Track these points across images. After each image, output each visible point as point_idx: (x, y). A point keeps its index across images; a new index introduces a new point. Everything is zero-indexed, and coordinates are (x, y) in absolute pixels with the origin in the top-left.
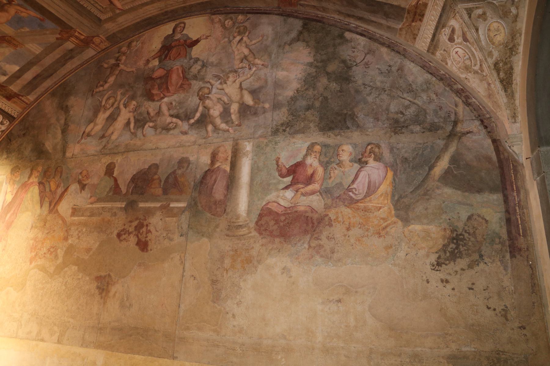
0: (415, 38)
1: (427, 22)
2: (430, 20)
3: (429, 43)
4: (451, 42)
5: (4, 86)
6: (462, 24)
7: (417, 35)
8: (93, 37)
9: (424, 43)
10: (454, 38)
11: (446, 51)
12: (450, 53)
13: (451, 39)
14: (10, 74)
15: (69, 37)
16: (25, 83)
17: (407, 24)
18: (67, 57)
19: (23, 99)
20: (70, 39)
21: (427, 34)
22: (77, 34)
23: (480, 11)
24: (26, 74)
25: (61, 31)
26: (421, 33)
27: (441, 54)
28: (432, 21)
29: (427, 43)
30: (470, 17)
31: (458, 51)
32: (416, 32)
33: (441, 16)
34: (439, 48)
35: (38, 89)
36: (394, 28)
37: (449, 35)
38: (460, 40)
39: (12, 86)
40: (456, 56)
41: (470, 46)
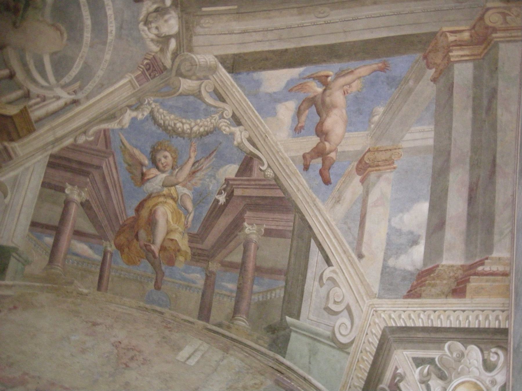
5: (430, 271)
8: (482, 18)
14: (423, 232)
15: (446, 56)
16: (463, 226)
18: (485, 102)
19: (487, 268)
20: (452, 59)
22: (451, 38)
24: (448, 206)
25: (425, 57)
35: (497, 219)
39: (445, 255)
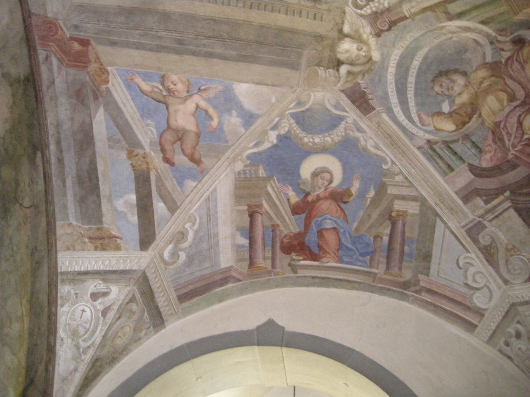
0: (68, 249)
1: (98, 257)
2: (103, 260)
3: (73, 269)
4: (91, 298)
6: (118, 300)
7: (74, 250)
9: (69, 263)
10: (98, 299)
11: (77, 297)
12: (77, 303)
13: (94, 296)
17: (82, 232)
21: (82, 263)
23: (134, 307)
26: (80, 254)
27: (69, 292)
28: (102, 263)
29: (71, 267)
30: (128, 303)
31: (86, 311)
32: (77, 247)
33: (114, 272)
34: (75, 287)
36: (68, 214)
37: (98, 291)
38: (100, 307)
40: (78, 312)
41: (101, 322)
